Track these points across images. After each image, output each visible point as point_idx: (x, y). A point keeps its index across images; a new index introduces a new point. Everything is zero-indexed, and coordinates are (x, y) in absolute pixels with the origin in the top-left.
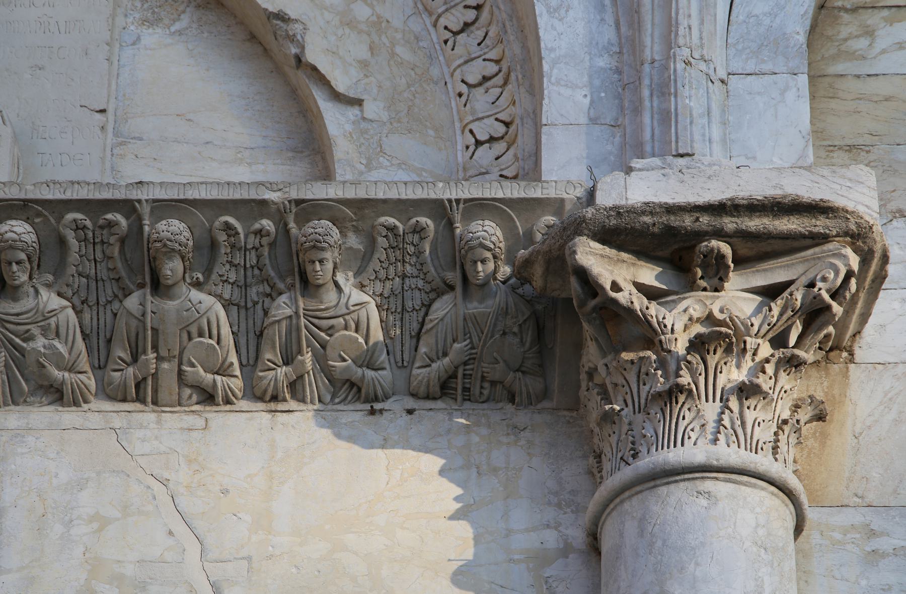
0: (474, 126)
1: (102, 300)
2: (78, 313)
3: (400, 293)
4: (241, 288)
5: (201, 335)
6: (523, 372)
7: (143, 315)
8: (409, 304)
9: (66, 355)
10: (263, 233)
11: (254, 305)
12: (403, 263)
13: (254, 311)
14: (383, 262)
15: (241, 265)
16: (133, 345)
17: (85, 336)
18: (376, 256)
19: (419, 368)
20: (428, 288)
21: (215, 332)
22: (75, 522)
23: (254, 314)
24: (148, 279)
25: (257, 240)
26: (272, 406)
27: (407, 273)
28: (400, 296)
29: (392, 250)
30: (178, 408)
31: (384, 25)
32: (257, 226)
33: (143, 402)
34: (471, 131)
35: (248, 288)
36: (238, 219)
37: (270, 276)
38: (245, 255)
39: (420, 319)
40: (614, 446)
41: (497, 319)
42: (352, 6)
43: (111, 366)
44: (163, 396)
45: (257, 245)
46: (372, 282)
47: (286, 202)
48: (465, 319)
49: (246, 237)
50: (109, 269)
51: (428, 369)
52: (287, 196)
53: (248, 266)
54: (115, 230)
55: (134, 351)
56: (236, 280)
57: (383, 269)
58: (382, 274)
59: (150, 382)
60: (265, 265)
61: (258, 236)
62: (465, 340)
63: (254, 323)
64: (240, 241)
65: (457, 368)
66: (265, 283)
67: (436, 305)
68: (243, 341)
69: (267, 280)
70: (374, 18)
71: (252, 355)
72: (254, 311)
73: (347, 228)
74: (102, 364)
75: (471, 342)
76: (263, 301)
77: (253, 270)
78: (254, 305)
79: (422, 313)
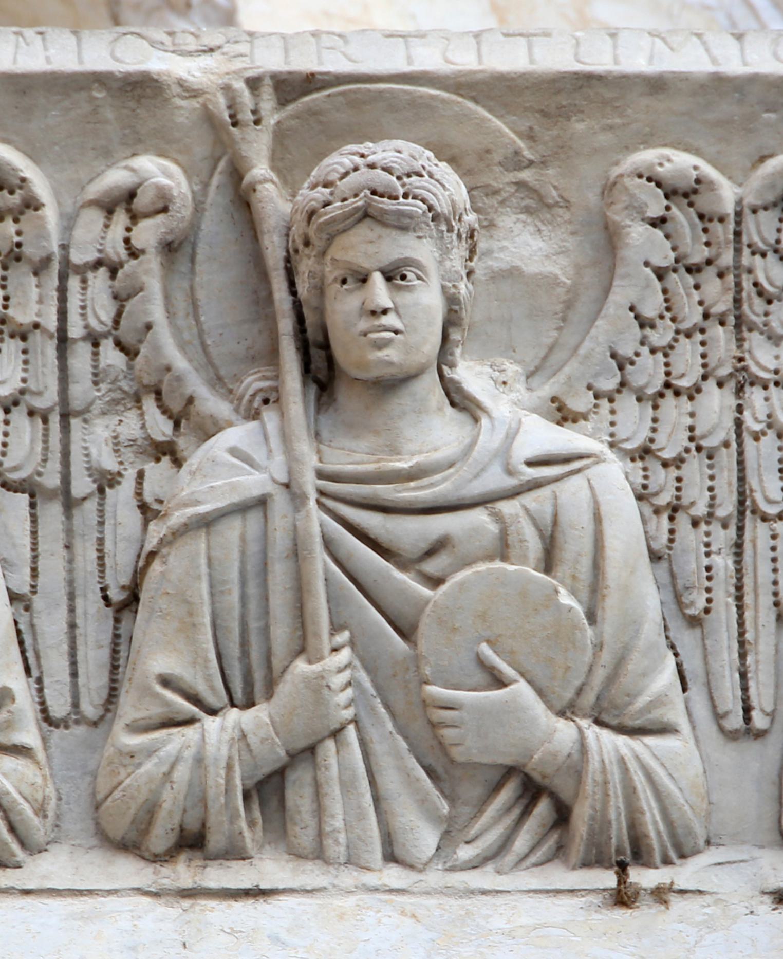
3: (726, 444)
4: (45, 421)
10: (142, 201)
11: (101, 491)
12: (738, 327)
13: (101, 512)
14: (653, 327)
15: (45, 331)
18: (621, 295)
23: (101, 523)
27: (754, 369)
28: (727, 458)
29: (690, 280)
35: (75, 423)
36: (33, 156)
37: (168, 369)
38: (62, 291)
45: (115, 249)
46: (604, 403)
47: (239, 85)
49: (69, 223)
52: (238, 64)
53: (75, 330)
56: (22, 392)
57: (653, 351)
60: (149, 327)
61: (121, 219)
63: (101, 558)
64: (42, 234)
66: (149, 404)
69: (158, 393)
72: (101, 512)
73: (496, 192)
76: (141, 475)
77: (96, 354)
78: (101, 491)
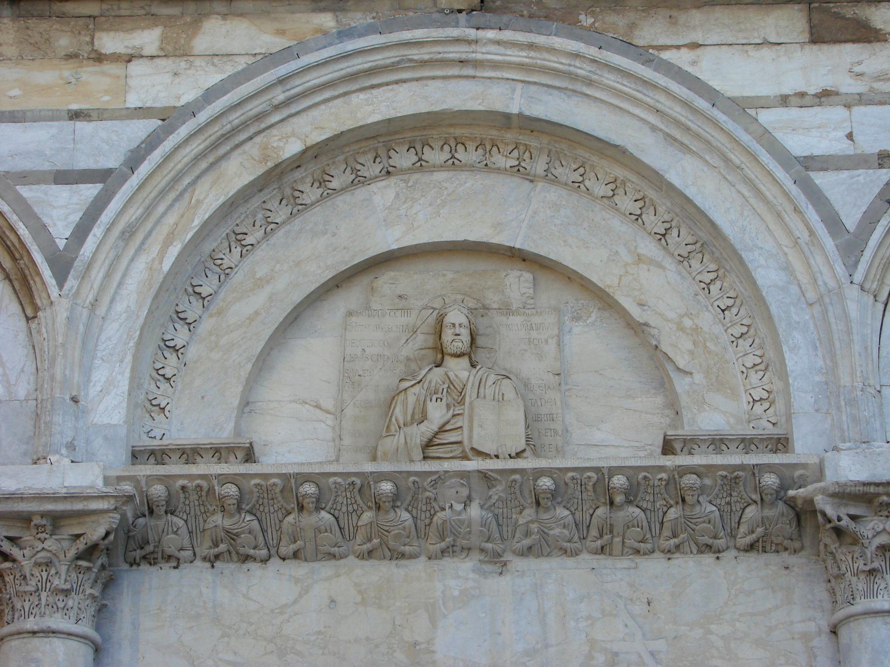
0: (752, 392)
1: (584, 509)
2: (573, 514)
5: (633, 527)
6: (792, 540)
7: (606, 518)
8: (734, 509)
9: (568, 535)
16: (601, 530)
17: (576, 525)
19: (740, 538)
20: (743, 501)
21: (640, 525)
22: (580, 620)
24: (608, 502)
25: (660, 483)
26: (668, 556)
30: (622, 557)
31: (699, 330)
32: (659, 476)
33: (605, 554)
34: (750, 394)
39: (740, 515)
40: (843, 590)
41: (778, 518)
42: (682, 319)
43: (589, 539)
44: (614, 553)
45: (660, 484)
48: (762, 518)
50: (588, 495)
51: (745, 539)
53: (655, 493)
54: (591, 479)
55: (601, 533)
58: (721, 496)
59: (608, 546)
62: (762, 526)
65: (759, 539)
67: (748, 510)
68: (653, 526)
70: (694, 326)
71: (658, 532)
74: (585, 536)
75: (766, 527)
79: (740, 513)
